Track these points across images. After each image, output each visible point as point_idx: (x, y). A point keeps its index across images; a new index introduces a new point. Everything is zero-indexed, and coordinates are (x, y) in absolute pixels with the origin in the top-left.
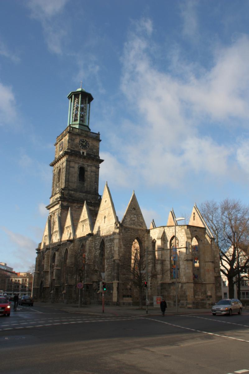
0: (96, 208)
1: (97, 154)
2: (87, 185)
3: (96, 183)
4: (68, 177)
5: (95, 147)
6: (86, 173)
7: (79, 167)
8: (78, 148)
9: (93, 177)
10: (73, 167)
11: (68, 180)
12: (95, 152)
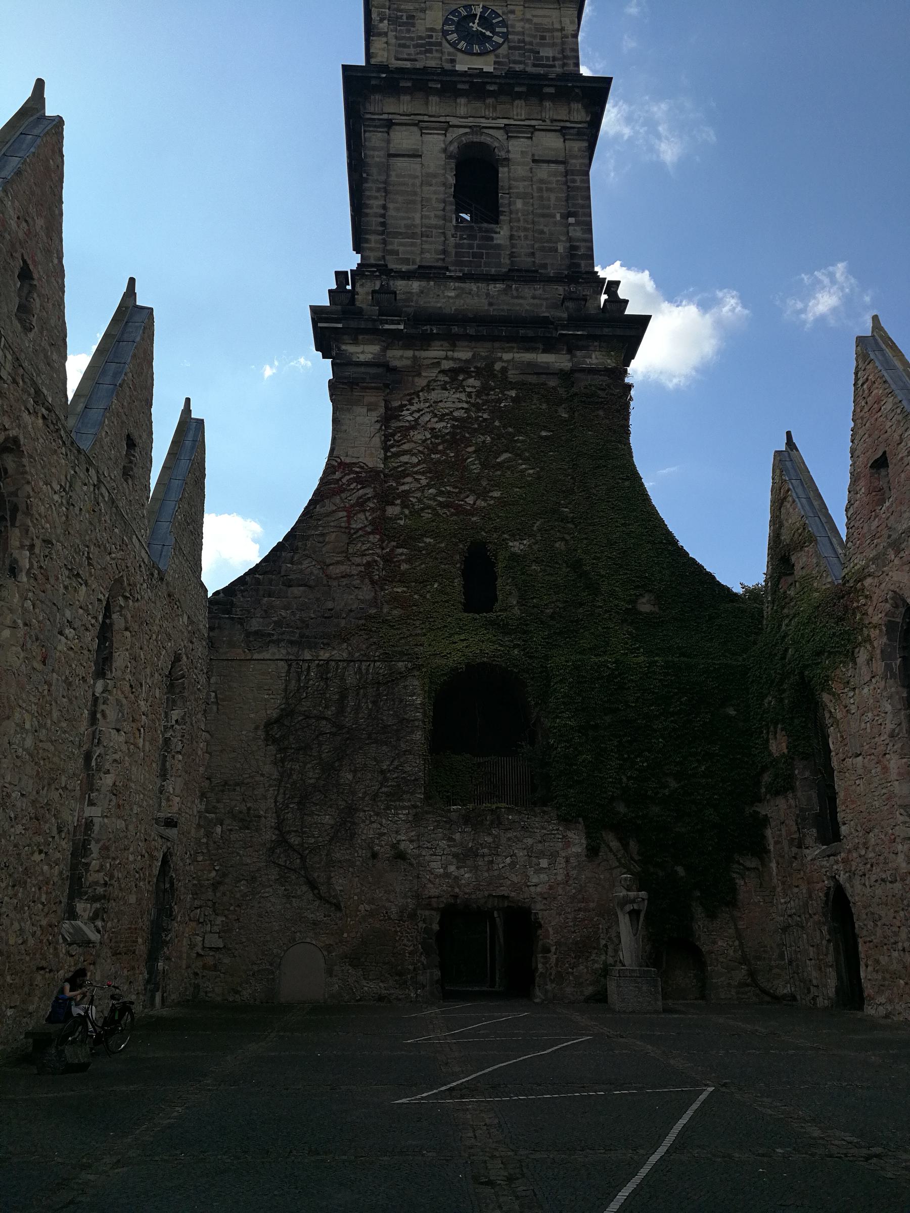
0: (578, 353)
1: (564, 65)
2: (512, 237)
3: (571, 220)
4: (384, 207)
5: (547, 35)
6: (503, 172)
7: (453, 148)
8: (436, 55)
9: (548, 190)
10: (416, 155)
11: (383, 224)
12: (554, 59)
